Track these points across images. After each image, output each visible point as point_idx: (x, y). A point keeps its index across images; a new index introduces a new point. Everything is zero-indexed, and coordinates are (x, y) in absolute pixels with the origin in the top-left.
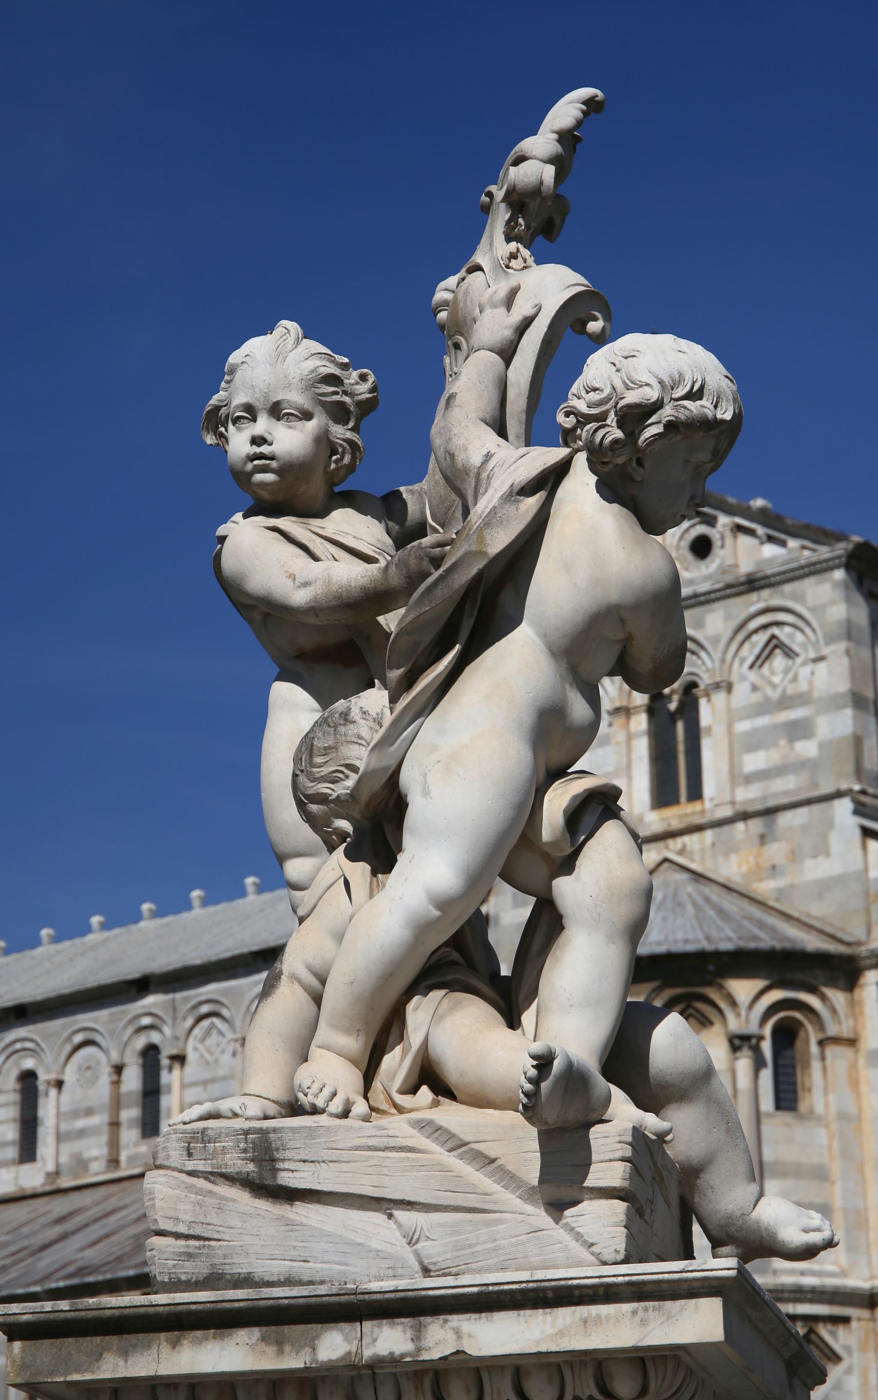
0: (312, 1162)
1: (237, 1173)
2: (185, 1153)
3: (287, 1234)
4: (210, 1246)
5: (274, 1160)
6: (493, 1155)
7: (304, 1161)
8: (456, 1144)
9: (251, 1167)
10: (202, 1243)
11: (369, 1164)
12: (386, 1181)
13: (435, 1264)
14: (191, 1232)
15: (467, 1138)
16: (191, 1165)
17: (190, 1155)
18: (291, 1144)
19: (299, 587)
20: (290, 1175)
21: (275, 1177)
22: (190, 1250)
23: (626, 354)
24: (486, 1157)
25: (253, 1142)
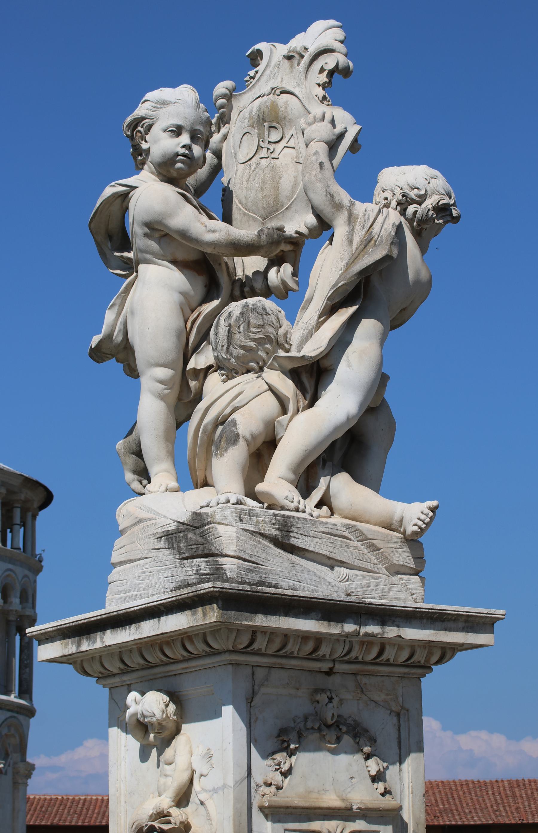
0: (305, 536)
1: (270, 534)
2: (238, 519)
3: (293, 568)
4: (260, 567)
5: (289, 531)
6: (380, 546)
7: (302, 534)
8: (363, 538)
9: (277, 533)
10: (255, 565)
11: (328, 541)
12: (335, 551)
13: (353, 592)
14: (251, 559)
15: (370, 537)
16: (243, 526)
17: (241, 520)
18: (297, 525)
19: (209, 231)
20: (295, 540)
21: (289, 540)
22: (251, 568)
23: (432, 176)
24: (376, 547)
25: (279, 520)
